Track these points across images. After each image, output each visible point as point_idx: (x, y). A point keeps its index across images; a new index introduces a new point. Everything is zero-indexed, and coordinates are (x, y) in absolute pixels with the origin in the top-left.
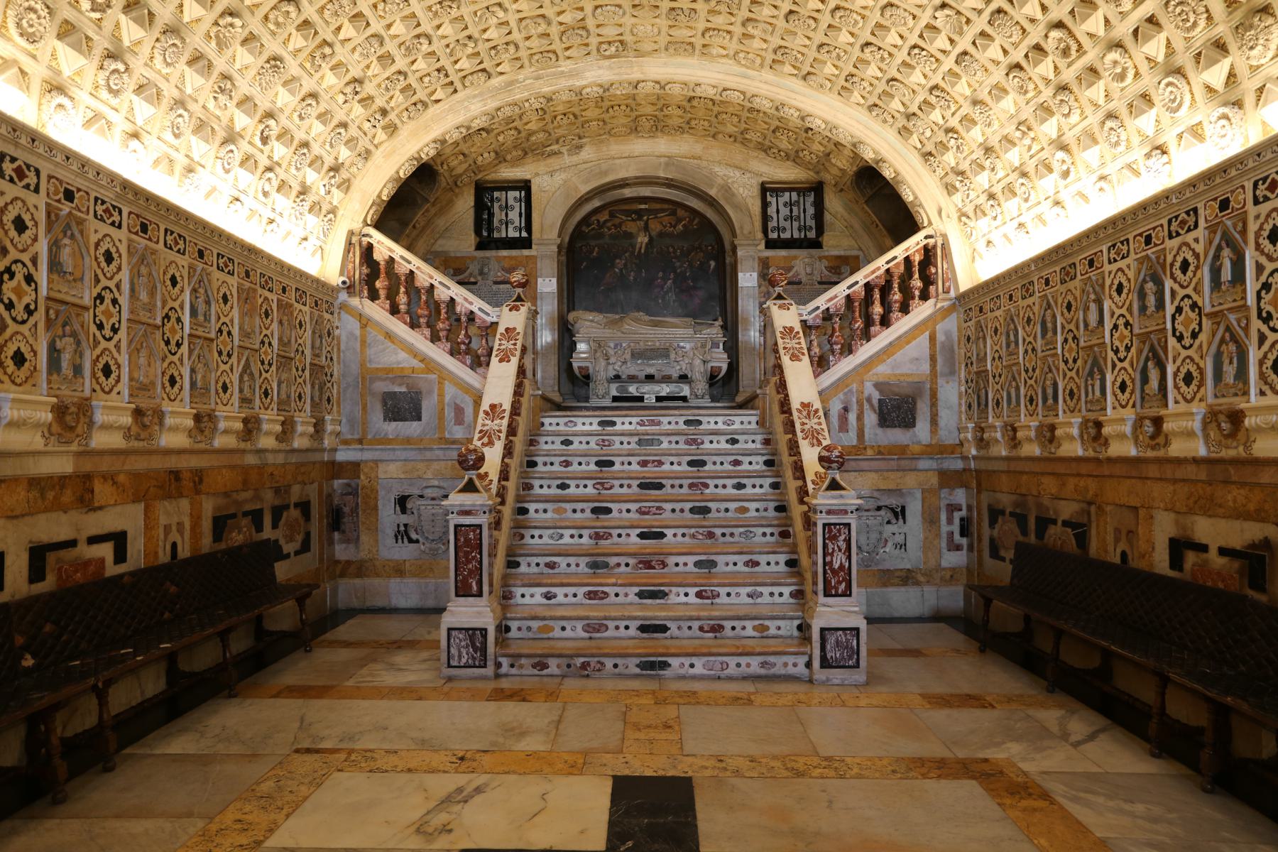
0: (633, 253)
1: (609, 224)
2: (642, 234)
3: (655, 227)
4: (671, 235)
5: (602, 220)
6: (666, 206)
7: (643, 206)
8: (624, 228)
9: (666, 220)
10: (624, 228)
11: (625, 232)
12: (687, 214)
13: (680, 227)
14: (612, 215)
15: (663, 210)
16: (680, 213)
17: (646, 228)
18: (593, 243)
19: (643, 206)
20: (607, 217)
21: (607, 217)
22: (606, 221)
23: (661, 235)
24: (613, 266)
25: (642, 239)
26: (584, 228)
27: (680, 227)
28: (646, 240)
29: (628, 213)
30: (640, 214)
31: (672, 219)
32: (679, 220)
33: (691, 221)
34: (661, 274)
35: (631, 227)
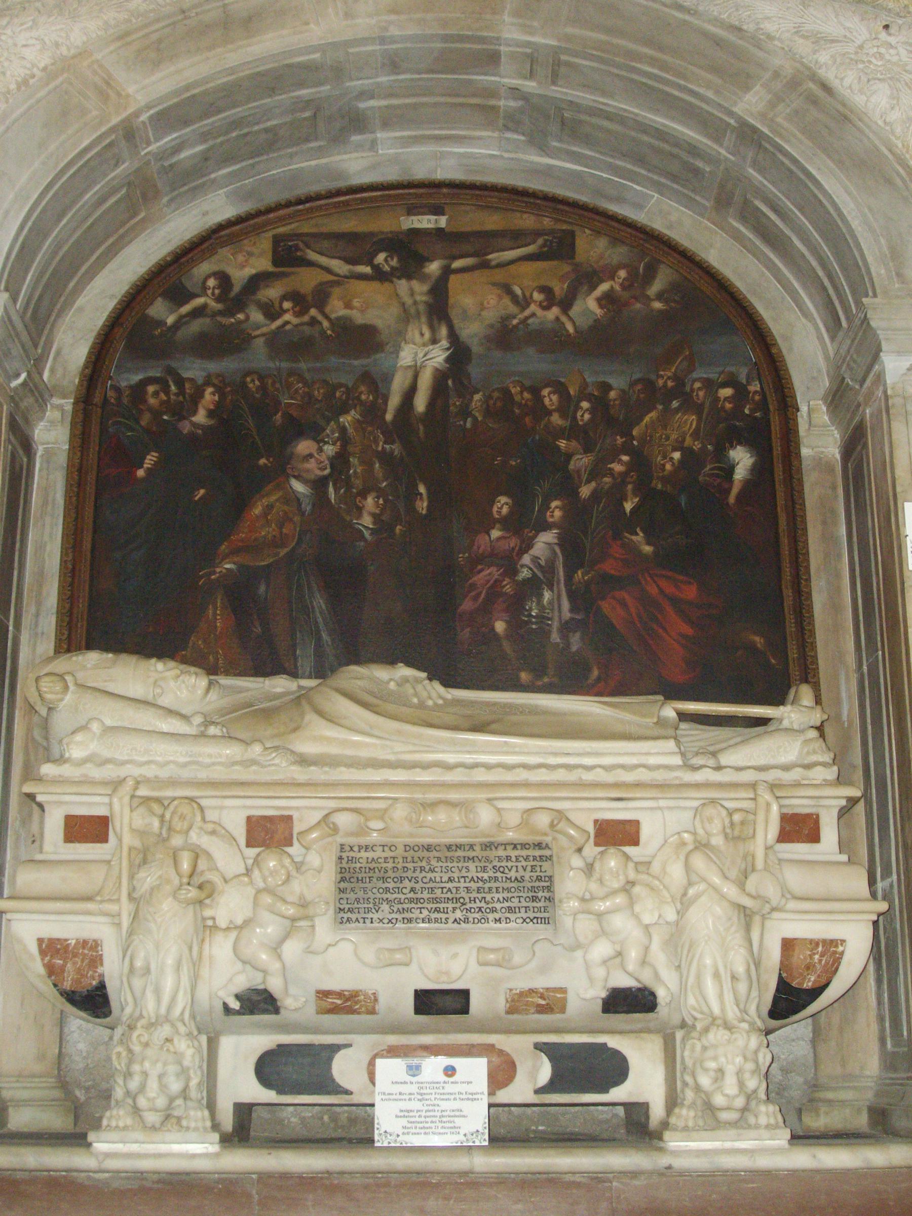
0: (373, 412)
1: (272, 292)
2: (418, 331)
3: (479, 306)
4: (552, 341)
5: (240, 275)
6: (527, 221)
7: (425, 222)
8: (337, 308)
9: (528, 277)
10: (337, 308)
11: (344, 328)
12: (618, 254)
13: (589, 306)
14: (287, 256)
15: (517, 237)
16: (592, 248)
17: (438, 309)
18: (194, 370)
19: (425, 222)
20: (263, 264)
21: (263, 264)
22: (256, 281)
23: (504, 336)
24: (283, 467)
25: (419, 357)
26: (161, 311)
27: (589, 306)
28: (438, 356)
29: (357, 247)
30: (409, 252)
31: (555, 274)
32: (587, 278)
33: (639, 280)
34: (502, 505)
35: (370, 304)
